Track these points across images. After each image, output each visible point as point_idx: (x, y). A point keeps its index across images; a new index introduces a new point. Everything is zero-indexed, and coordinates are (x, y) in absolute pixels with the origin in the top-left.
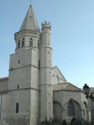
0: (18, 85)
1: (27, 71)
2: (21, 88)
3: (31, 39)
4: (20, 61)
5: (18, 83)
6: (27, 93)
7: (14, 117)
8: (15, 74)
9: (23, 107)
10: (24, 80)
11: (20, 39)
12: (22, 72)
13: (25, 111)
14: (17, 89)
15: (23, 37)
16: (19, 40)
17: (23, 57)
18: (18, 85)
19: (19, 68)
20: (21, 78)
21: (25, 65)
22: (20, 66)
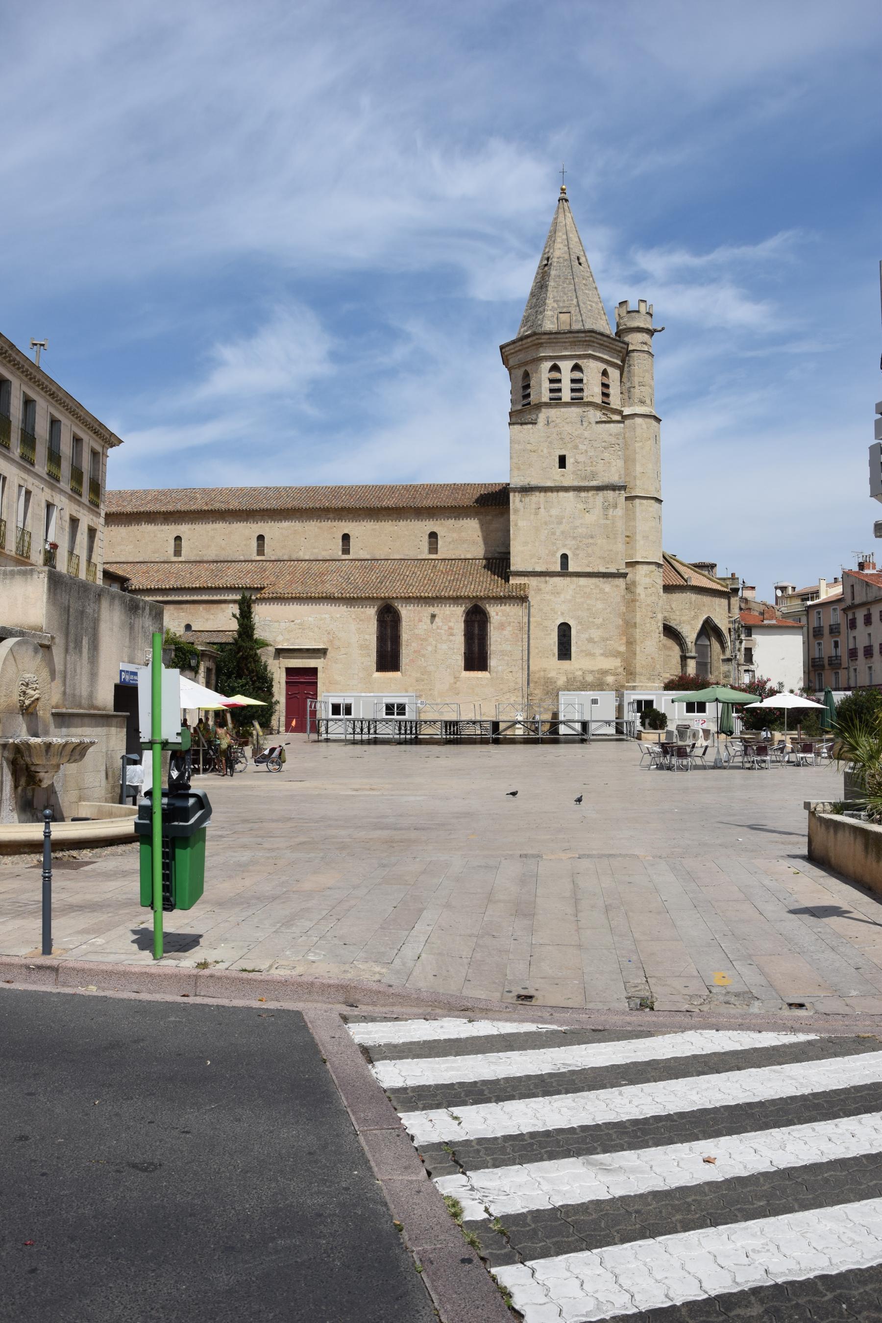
0: (564, 557)
1: (606, 509)
2: (579, 570)
3: (605, 373)
4: (569, 462)
5: (564, 546)
6: (607, 590)
7: (553, 674)
8: (542, 510)
9: (590, 640)
10: (591, 541)
11: (557, 363)
12: (581, 506)
13: (602, 655)
14: (558, 569)
15: (580, 362)
16: (555, 368)
17: (581, 446)
18: (564, 557)
19: (566, 489)
20: (576, 527)
21: (594, 483)
22: (567, 477)
